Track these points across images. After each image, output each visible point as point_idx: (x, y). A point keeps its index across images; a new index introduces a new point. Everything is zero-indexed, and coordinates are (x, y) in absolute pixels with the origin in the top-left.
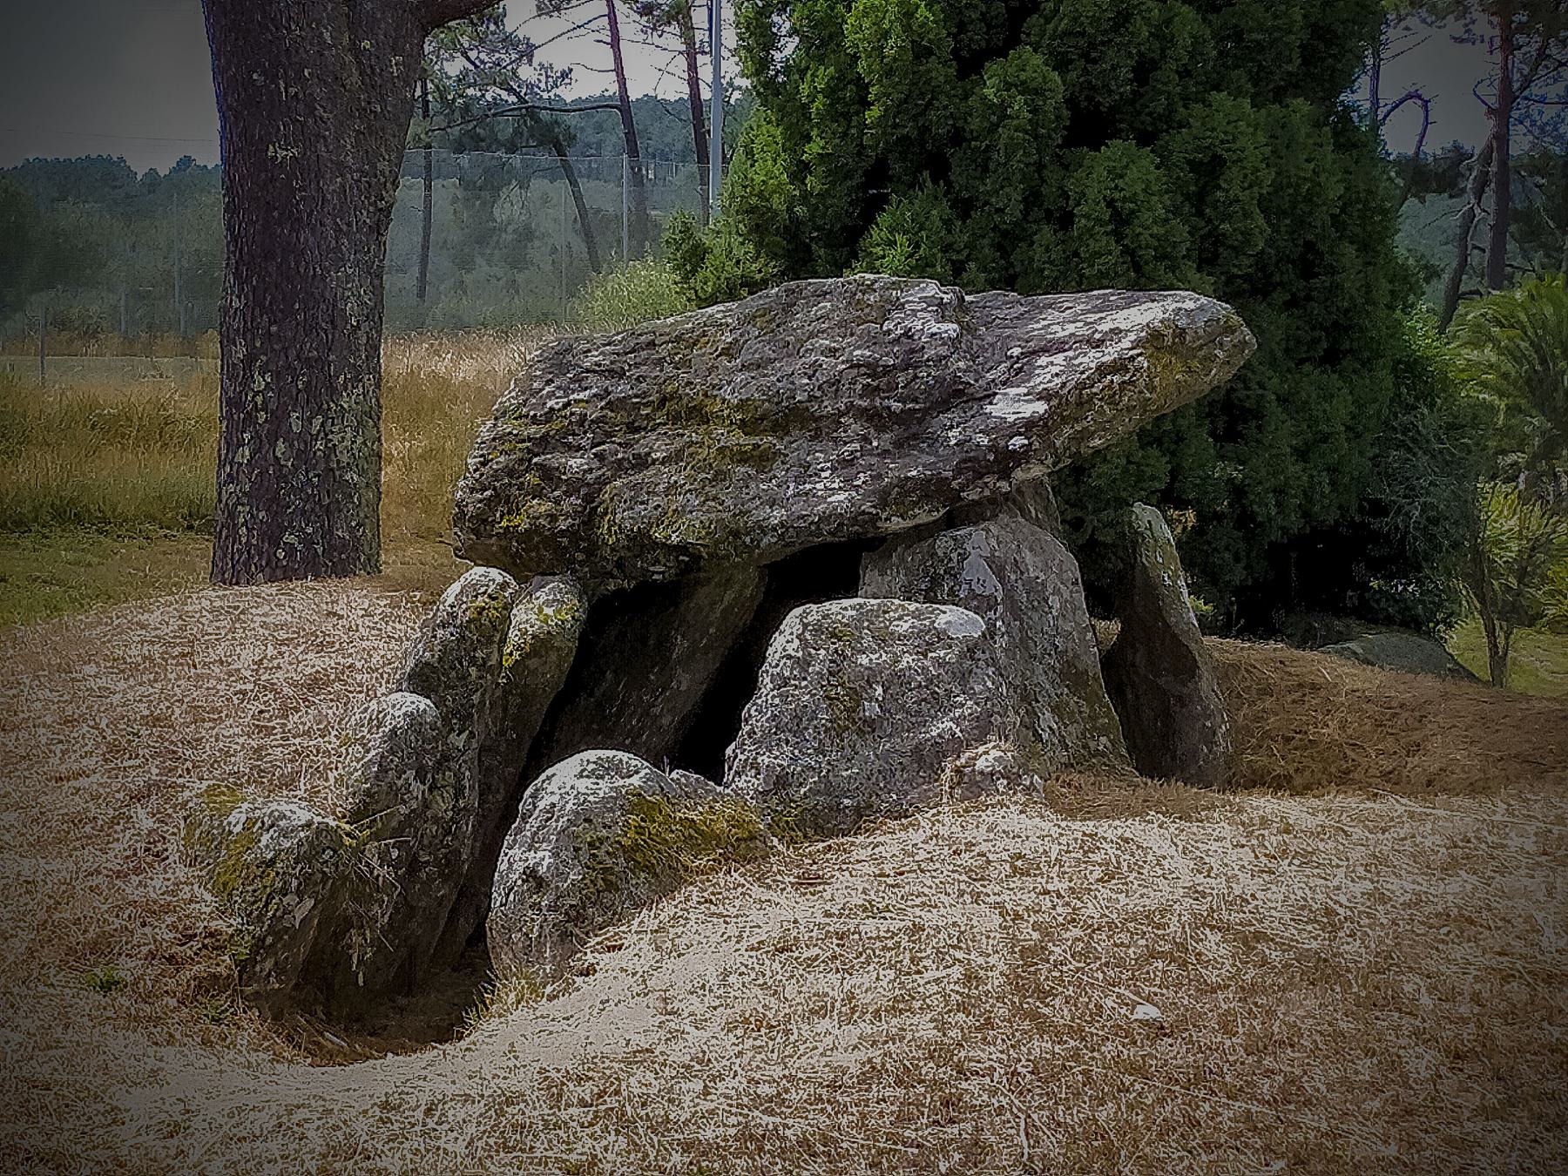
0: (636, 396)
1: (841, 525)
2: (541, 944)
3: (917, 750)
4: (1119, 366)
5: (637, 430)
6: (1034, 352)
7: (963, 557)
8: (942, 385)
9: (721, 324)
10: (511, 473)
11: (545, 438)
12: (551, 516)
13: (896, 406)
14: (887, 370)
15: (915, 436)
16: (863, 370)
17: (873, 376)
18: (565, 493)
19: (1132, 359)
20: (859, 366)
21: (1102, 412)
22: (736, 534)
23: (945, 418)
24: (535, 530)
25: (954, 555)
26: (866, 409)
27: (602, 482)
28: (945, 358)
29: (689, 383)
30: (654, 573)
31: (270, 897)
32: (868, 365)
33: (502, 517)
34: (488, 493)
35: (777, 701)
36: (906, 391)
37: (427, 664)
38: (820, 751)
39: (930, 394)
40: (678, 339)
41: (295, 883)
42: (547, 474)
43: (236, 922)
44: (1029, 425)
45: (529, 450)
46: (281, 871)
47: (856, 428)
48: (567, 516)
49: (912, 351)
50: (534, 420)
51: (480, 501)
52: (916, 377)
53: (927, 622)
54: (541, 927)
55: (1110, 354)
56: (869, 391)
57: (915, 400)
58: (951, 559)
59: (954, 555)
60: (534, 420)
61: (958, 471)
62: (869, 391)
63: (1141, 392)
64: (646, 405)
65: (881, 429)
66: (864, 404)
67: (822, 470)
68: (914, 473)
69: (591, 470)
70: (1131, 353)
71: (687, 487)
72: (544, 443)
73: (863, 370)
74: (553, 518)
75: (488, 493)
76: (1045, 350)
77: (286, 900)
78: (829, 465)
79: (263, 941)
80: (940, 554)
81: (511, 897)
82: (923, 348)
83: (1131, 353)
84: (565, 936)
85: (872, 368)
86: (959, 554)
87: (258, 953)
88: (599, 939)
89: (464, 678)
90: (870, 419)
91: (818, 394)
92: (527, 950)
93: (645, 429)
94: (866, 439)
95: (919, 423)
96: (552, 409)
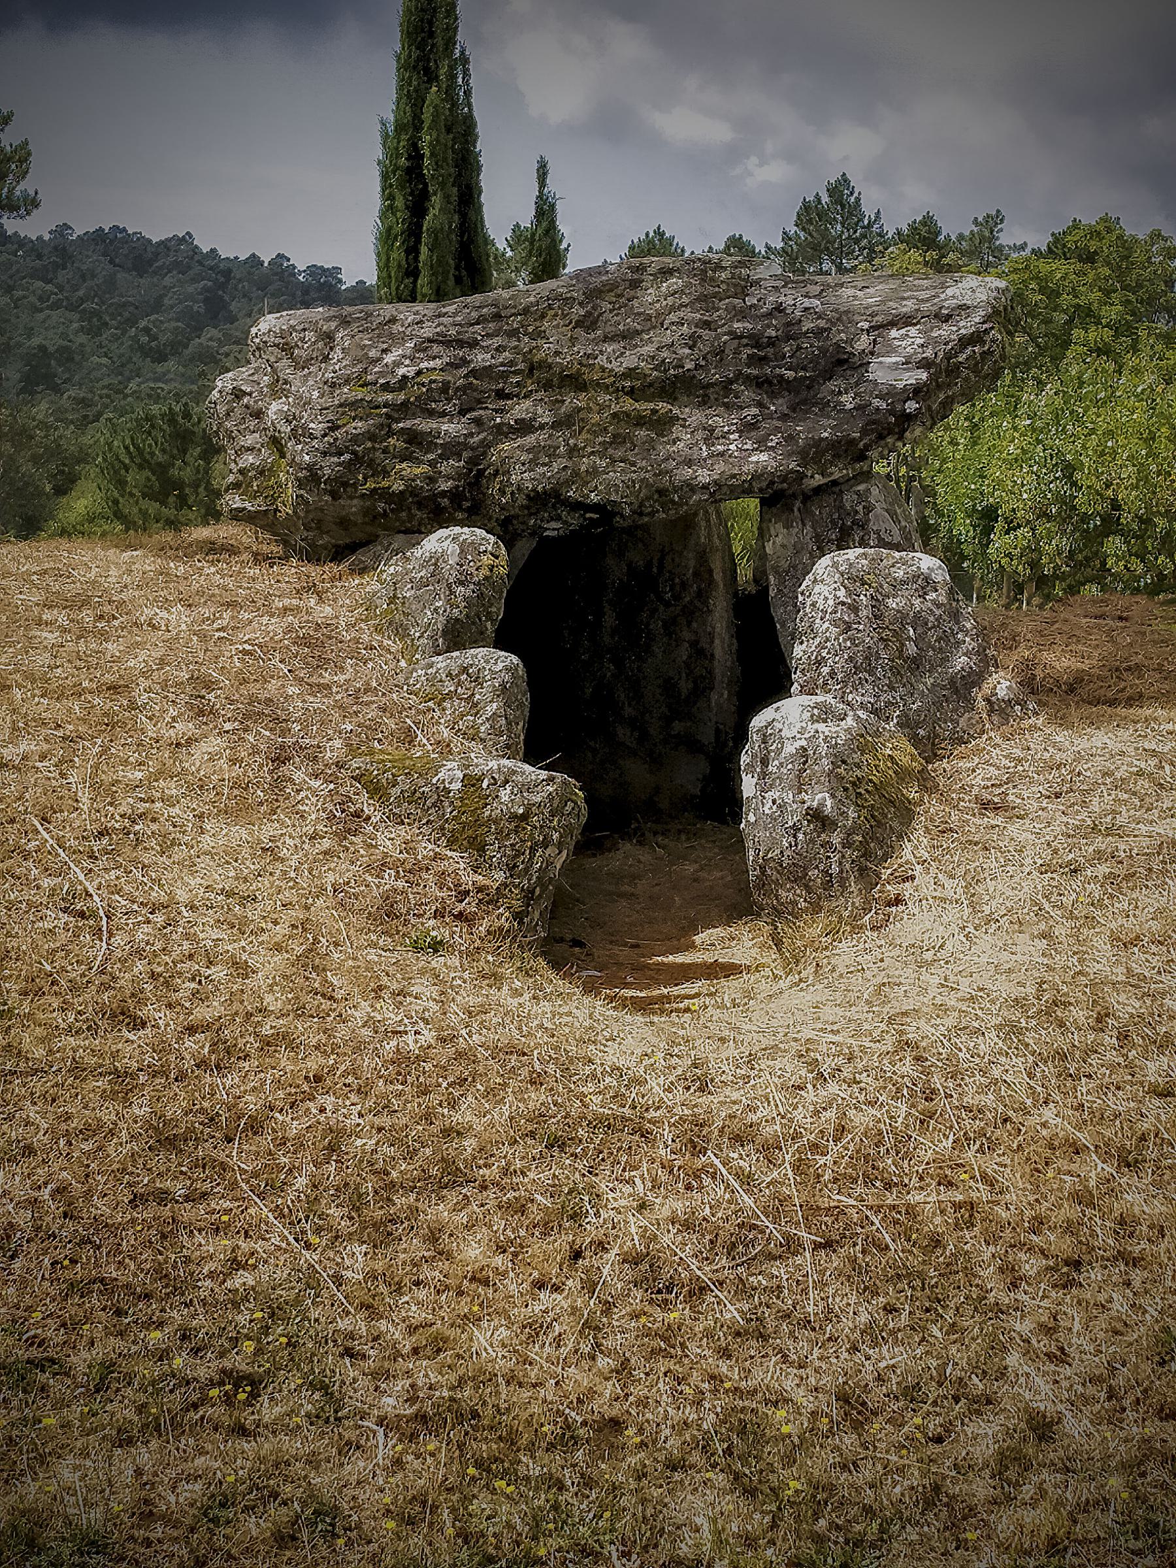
0: (502, 365)
1: (772, 483)
2: (843, 882)
3: (952, 682)
4: (975, 338)
5: (508, 397)
6: (881, 326)
7: (868, 509)
8: (825, 355)
9: (567, 299)
10: (372, 437)
11: (405, 404)
12: (430, 478)
13: (790, 374)
14: (772, 342)
15: (804, 402)
16: (745, 341)
17: (758, 345)
18: (440, 456)
19: (986, 331)
20: (741, 337)
21: (967, 379)
22: (662, 492)
23: (832, 385)
24: (411, 491)
25: (860, 508)
26: (757, 377)
27: (486, 445)
28: (826, 330)
29: (557, 353)
30: (547, 529)
31: (533, 850)
32: (751, 336)
33: (365, 478)
34: (347, 457)
35: (848, 644)
36: (794, 360)
37: (457, 620)
38: (892, 688)
39: (818, 363)
40: (526, 311)
41: (556, 836)
42: (414, 438)
43: (500, 876)
44: (917, 391)
45: (388, 416)
46: (537, 824)
47: (748, 395)
48: (448, 477)
49: (789, 324)
50: (386, 387)
51: (339, 464)
52: (799, 348)
53: (914, 568)
54: (840, 863)
55: (967, 326)
56: (753, 360)
57: (804, 369)
58: (857, 512)
59: (860, 508)
60: (386, 387)
61: (864, 432)
62: (753, 360)
63: (996, 361)
64: (515, 373)
65: (773, 396)
66: (755, 372)
67: (729, 432)
68: (826, 435)
69: (471, 435)
70: (985, 326)
71: (589, 450)
72: (404, 409)
73: (745, 341)
74: (431, 480)
75: (347, 457)
76: (892, 324)
77: (548, 852)
78: (734, 428)
79: (533, 892)
80: (848, 506)
81: (801, 836)
82: (800, 321)
83: (985, 326)
84: (863, 870)
85: (755, 340)
86: (864, 507)
87: (528, 905)
88: (889, 871)
89: (482, 633)
90: (759, 385)
91: (703, 363)
92: (828, 885)
93: (517, 396)
94: (760, 405)
95: (809, 388)
96: (404, 377)
